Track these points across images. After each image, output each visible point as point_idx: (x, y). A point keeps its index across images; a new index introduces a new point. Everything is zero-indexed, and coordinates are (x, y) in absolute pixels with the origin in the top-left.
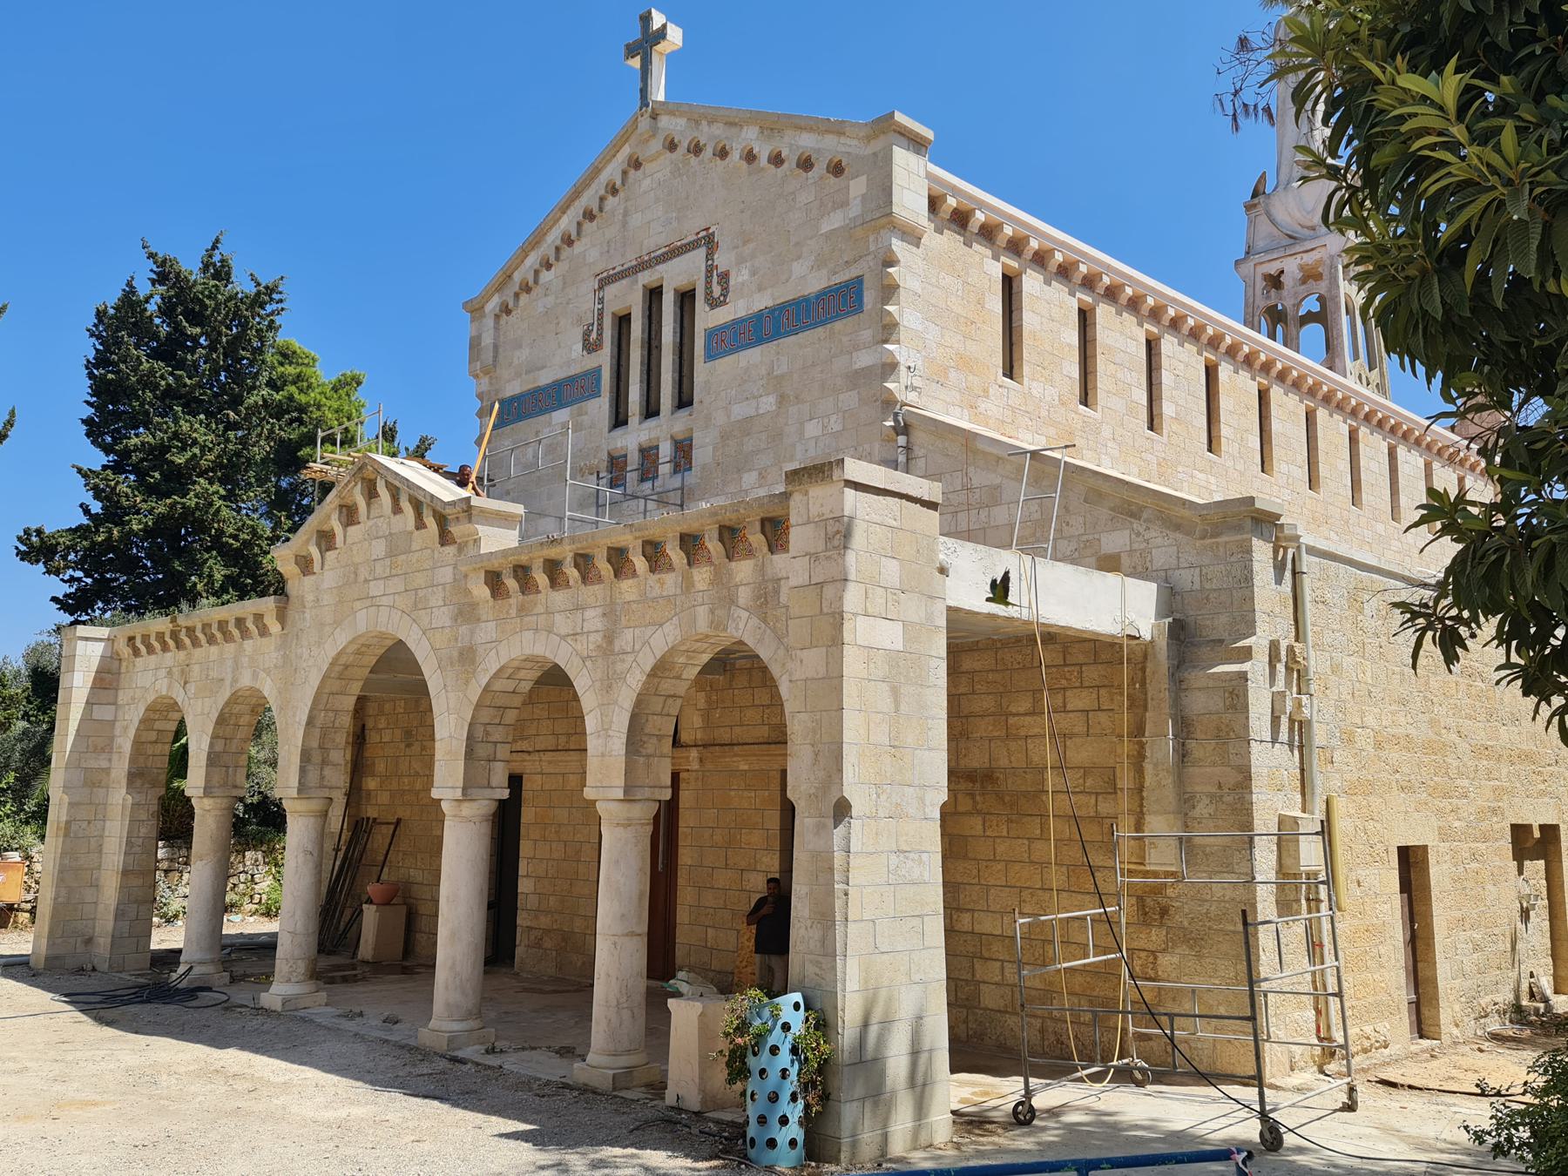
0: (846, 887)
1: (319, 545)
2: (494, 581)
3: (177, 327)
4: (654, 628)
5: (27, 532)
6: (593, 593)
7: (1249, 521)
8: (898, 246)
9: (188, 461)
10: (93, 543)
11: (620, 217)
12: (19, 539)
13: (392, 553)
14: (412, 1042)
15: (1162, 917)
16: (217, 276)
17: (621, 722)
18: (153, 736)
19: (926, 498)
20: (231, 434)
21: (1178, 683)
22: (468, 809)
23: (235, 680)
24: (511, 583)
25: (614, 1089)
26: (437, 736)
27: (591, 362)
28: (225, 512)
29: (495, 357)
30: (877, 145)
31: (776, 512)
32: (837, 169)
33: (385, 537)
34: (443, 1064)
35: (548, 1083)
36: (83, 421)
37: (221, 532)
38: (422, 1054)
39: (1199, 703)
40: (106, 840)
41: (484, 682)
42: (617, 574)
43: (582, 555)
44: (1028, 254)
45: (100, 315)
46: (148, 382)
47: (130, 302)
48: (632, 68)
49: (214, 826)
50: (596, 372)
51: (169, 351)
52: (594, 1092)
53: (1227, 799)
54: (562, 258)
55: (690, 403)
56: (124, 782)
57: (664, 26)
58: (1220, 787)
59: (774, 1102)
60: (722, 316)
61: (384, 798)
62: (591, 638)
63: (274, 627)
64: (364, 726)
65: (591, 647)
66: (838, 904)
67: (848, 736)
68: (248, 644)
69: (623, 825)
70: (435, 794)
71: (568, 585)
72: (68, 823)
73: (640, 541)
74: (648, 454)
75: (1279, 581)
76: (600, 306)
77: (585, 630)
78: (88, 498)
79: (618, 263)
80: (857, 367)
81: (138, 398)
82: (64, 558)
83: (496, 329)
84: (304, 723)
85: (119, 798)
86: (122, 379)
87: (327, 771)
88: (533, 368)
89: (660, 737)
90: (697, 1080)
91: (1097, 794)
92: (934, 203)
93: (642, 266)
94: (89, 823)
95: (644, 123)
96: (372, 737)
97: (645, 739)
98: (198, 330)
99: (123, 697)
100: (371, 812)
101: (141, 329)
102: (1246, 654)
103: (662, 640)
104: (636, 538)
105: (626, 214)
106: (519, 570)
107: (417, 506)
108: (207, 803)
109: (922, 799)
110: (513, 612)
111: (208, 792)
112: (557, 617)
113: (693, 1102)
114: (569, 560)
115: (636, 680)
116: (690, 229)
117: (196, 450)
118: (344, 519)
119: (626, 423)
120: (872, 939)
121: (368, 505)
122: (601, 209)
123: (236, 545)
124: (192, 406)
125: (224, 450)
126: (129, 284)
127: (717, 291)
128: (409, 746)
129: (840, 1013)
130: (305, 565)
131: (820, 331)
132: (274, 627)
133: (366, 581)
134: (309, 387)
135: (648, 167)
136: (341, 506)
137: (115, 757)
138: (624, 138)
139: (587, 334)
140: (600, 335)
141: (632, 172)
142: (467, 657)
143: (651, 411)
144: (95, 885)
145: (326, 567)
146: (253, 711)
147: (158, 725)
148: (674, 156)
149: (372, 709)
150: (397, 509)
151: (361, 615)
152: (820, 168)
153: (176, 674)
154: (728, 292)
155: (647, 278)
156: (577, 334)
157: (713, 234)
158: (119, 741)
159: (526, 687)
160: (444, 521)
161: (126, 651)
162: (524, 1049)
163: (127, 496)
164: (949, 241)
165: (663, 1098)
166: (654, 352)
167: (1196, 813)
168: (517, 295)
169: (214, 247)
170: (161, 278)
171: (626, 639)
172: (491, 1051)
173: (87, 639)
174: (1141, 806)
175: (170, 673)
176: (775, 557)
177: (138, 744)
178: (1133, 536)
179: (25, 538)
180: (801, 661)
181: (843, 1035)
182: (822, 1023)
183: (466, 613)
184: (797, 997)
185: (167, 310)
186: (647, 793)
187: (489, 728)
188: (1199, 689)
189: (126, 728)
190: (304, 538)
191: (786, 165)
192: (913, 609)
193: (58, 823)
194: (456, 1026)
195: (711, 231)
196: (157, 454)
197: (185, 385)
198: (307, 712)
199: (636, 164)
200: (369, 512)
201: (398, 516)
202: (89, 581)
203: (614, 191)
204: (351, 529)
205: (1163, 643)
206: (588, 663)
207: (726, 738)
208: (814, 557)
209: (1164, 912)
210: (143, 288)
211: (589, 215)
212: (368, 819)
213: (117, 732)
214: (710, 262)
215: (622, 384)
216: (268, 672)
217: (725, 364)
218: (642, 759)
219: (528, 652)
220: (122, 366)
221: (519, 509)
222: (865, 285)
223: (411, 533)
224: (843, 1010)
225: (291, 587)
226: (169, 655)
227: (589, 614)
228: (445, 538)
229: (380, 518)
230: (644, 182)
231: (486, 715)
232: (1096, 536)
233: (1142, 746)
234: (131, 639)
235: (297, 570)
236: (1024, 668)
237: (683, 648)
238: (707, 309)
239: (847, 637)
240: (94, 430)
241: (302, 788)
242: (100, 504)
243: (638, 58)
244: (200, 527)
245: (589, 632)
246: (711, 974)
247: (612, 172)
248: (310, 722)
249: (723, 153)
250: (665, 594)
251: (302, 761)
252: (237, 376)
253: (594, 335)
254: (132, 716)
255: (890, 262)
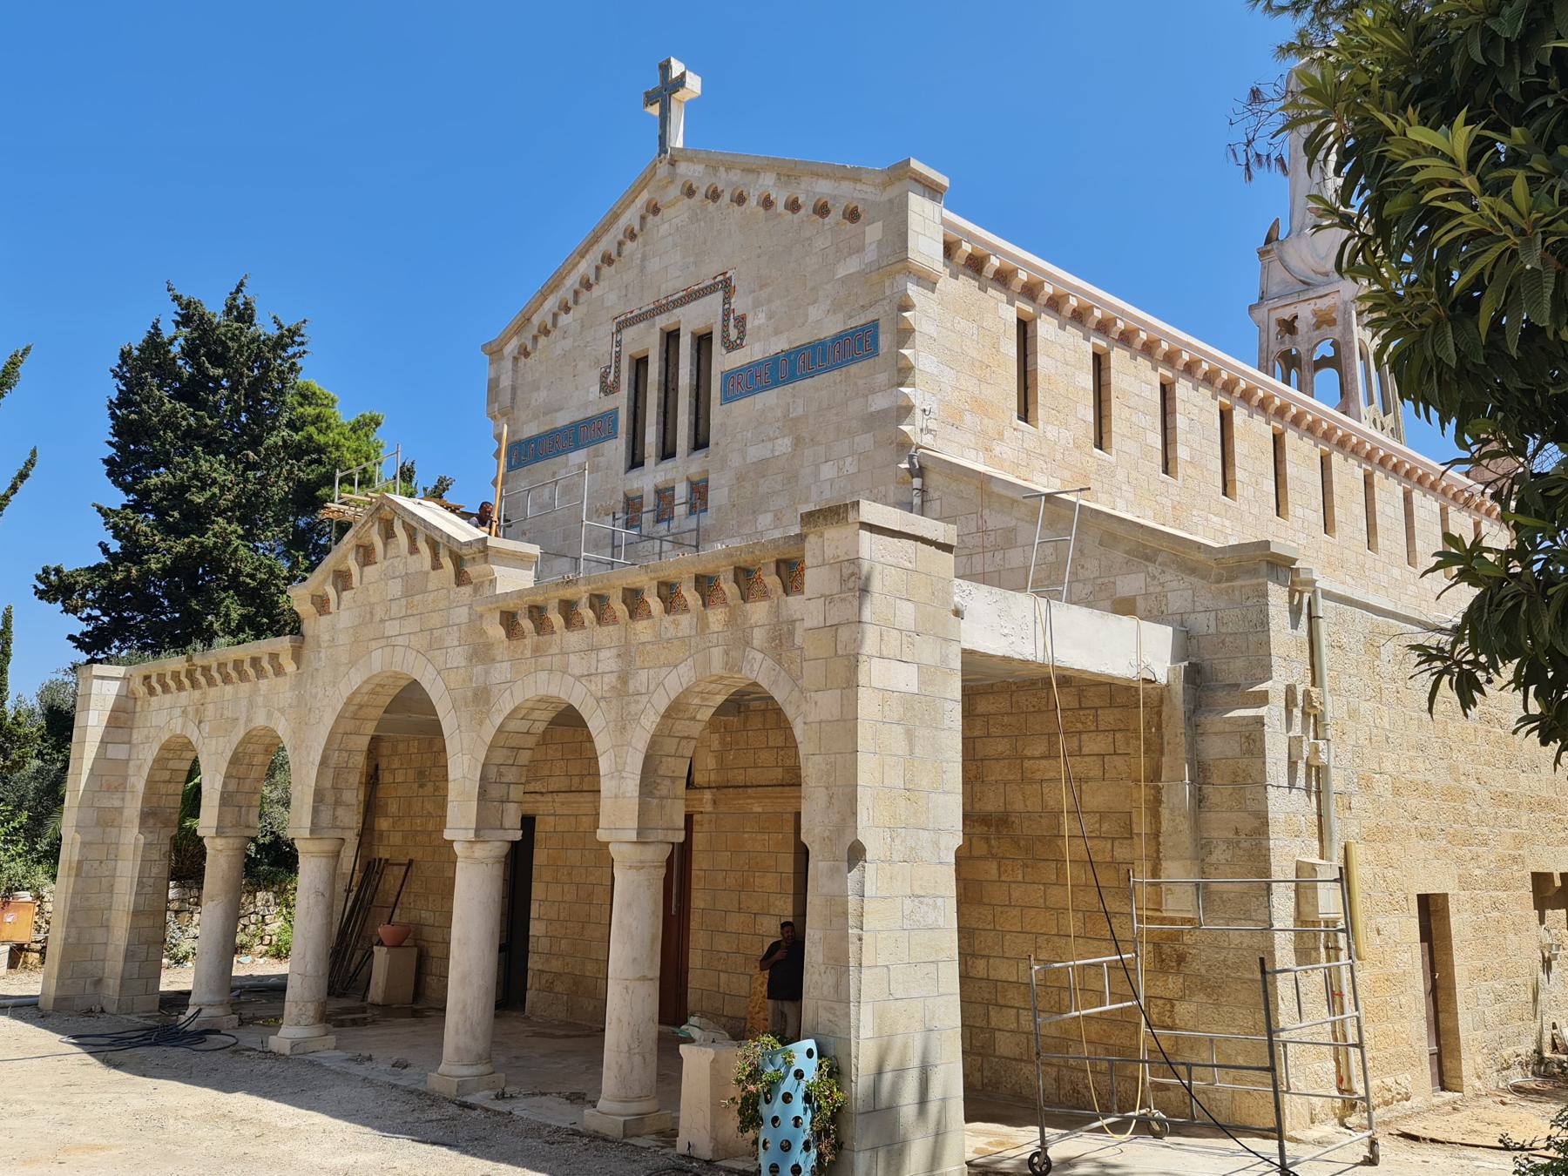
0: (860, 932)
1: (335, 585)
2: (509, 621)
3: (200, 368)
4: (669, 669)
5: (46, 571)
6: (607, 634)
7: (1264, 565)
8: (913, 290)
9: (207, 500)
10: (111, 582)
11: (638, 262)
12: (38, 577)
13: (408, 593)
14: (421, 1087)
15: (1179, 965)
16: (240, 318)
17: (635, 762)
18: (166, 775)
19: (941, 540)
20: (250, 474)
21: (1194, 728)
22: (481, 851)
23: (249, 720)
24: (526, 624)
25: (625, 1136)
26: (451, 777)
27: (608, 403)
28: (242, 552)
29: (513, 399)
30: (892, 192)
31: (790, 553)
32: (853, 215)
33: (401, 577)
34: (452, 1110)
35: (558, 1129)
36: (105, 462)
37: (238, 572)
38: (431, 1099)
39: (1216, 748)
40: (117, 880)
41: (498, 722)
42: (633, 615)
43: (598, 596)
44: (1043, 299)
45: (125, 356)
46: (169, 422)
47: (154, 344)
48: (651, 116)
49: (225, 866)
50: (615, 411)
51: (190, 393)
52: (605, 1139)
53: (1244, 845)
54: (581, 301)
55: (706, 445)
56: (137, 821)
57: (683, 75)
58: (1237, 833)
59: (786, 1151)
60: (738, 359)
61: (396, 839)
63: (290, 667)
64: (377, 766)
65: (606, 688)
66: (852, 949)
67: (863, 779)
68: (263, 684)
69: (636, 867)
70: (448, 835)
71: (583, 626)
72: (80, 862)
73: (655, 582)
74: (664, 495)
75: (1295, 625)
76: (618, 349)
77: (599, 671)
78: (108, 537)
79: (637, 305)
80: (873, 409)
81: (159, 438)
82: (82, 596)
83: (515, 370)
84: (317, 763)
85: (131, 837)
86: (144, 419)
87: (340, 811)
88: (550, 410)
89: (673, 779)
90: (708, 1128)
91: (1113, 839)
92: (949, 249)
93: (660, 309)
94: (101, 863)
95: (663, 169)
96: (386, 777)
97: (659, 781)
98: (221, 371)
99: (137, 736)
100: (383, 853)
101: (165, 370)
102: (1263, 698)
103: (676, 681)
104: (651, 579)
105: (644, 259)
106: (535, 610)
107: (434, 546)
108: (220, 843)
109: (936, 844)
110: (528, 653)
111: (220, 832)
112: (572, 657)
113: (704, 1150)
114: (584, 600)
115: (650, 722)
116: (707, 273)
117: (216, 490)
118: (361, 559)
119: (642, 464)
120: (886, 985)
121: (385, 545)
122: (619, 254)
123: (253, 584)
124: (212, 447)
125: (243, 490)
126: (155, 326)
127: (733, 334)
128: (421, 786)
129: (854, 1061)
130: (321, 604)
131: (836, 375)
132: (290, 667)
133: (382, 621)
134: (328, 427)
135: (666, 213)
136: (358, 546)
137: (128, 796)
138: (643, 184)
139: (604, 376)
140: (617, 377)
141: (650, 218)
142: (481, 698)
143: (667, 453)
144: (106, 927)
145: (342, 607)
146: (267, 751)
147: (172, 764)
148: (692, 201)
149: (385, 748)
150: (414, 549)
151: (377, 656)
152: (836, 214)
153: (191, 715)
154: (744, 336)
155: (664, 321)
157: (730, 278)
158: (133, 779)
159: (540, 727)
160: (460, 561)
161: (141, 690)
162: (534, 1094)
163: (146, 535)
164: (962, 287)
165: (675, 1146)
166: (671, 394)
167: (1213, 859)
168: (535, 338)
169: (238, 290)
170: (185, 320)
171: (640, 680)
172: (501, 1096)
173: (103, 678)
174: (1158, 851)
175: (184, 712)
176: (790, 599)
177: (151, 783)
178: (1148, 580)
179: (44, 576)
180: (816, 703)
181: (856, 1083)
182: (835, 1070)
183: (481, 653)
184: (810, 1044)
185: (190, 352)
186: (660, 835)
187: (503, 769)
188: (1215, 733)
189: (140, 767)
190: (321, 577)
191: (802, 211)
192: (928, 651)
193: (70, 862)
194: (466, 1071)
195: (728, 275)
196: (177, 493)
197: (206, 426)
198: (321, 751)
199: (655, 210)
200: (385, 552)
201: (415, 557)
202: (106, 619)
203: (632, 236)
204: (368, 569)
205: (1179, 687)
206: (603, 704)
207: (740, 780)
208: (828, 598)
209: (1181, 959)
210: (168, 330)
211: (608, 260)
212: (380, 859)
213: (131, 771)
214: (727, 306)
215: (638, 426)
216: (282, 711)
217: (741, 407)
218: (655, 801)
219: (542, 692)
220: (145, 407)
221: (535, 550)
222: (881, 329)
223: (427, 573)
224: (857, 1057)
225: (307, 627)
226: (183, 694)
227: (604, 654)
228: (461, 578)
229: (397, 558)
230: (662, 227)
231: (500, 756)
232: (1112, 580)
233: (1158, 790)
234: (147, 678)
235: (314, 610)
236: (1039, 711)
237: (697, 689)
238: (724, 351)
239: (862, 679)
240: (115, 469)
241: (314, 828)
242: (120, 544)
243: (658, 105)
244: (218, 566)
245: (603, 673)
246: (724, 1020)
247: (630, 217)
248: (324, 762)
249: (740, 199)
250: (680, 635)
251: (314, 801)
252: (257, 416)
253: (611, 378)
254: (147, 754)
255: (906, 306)
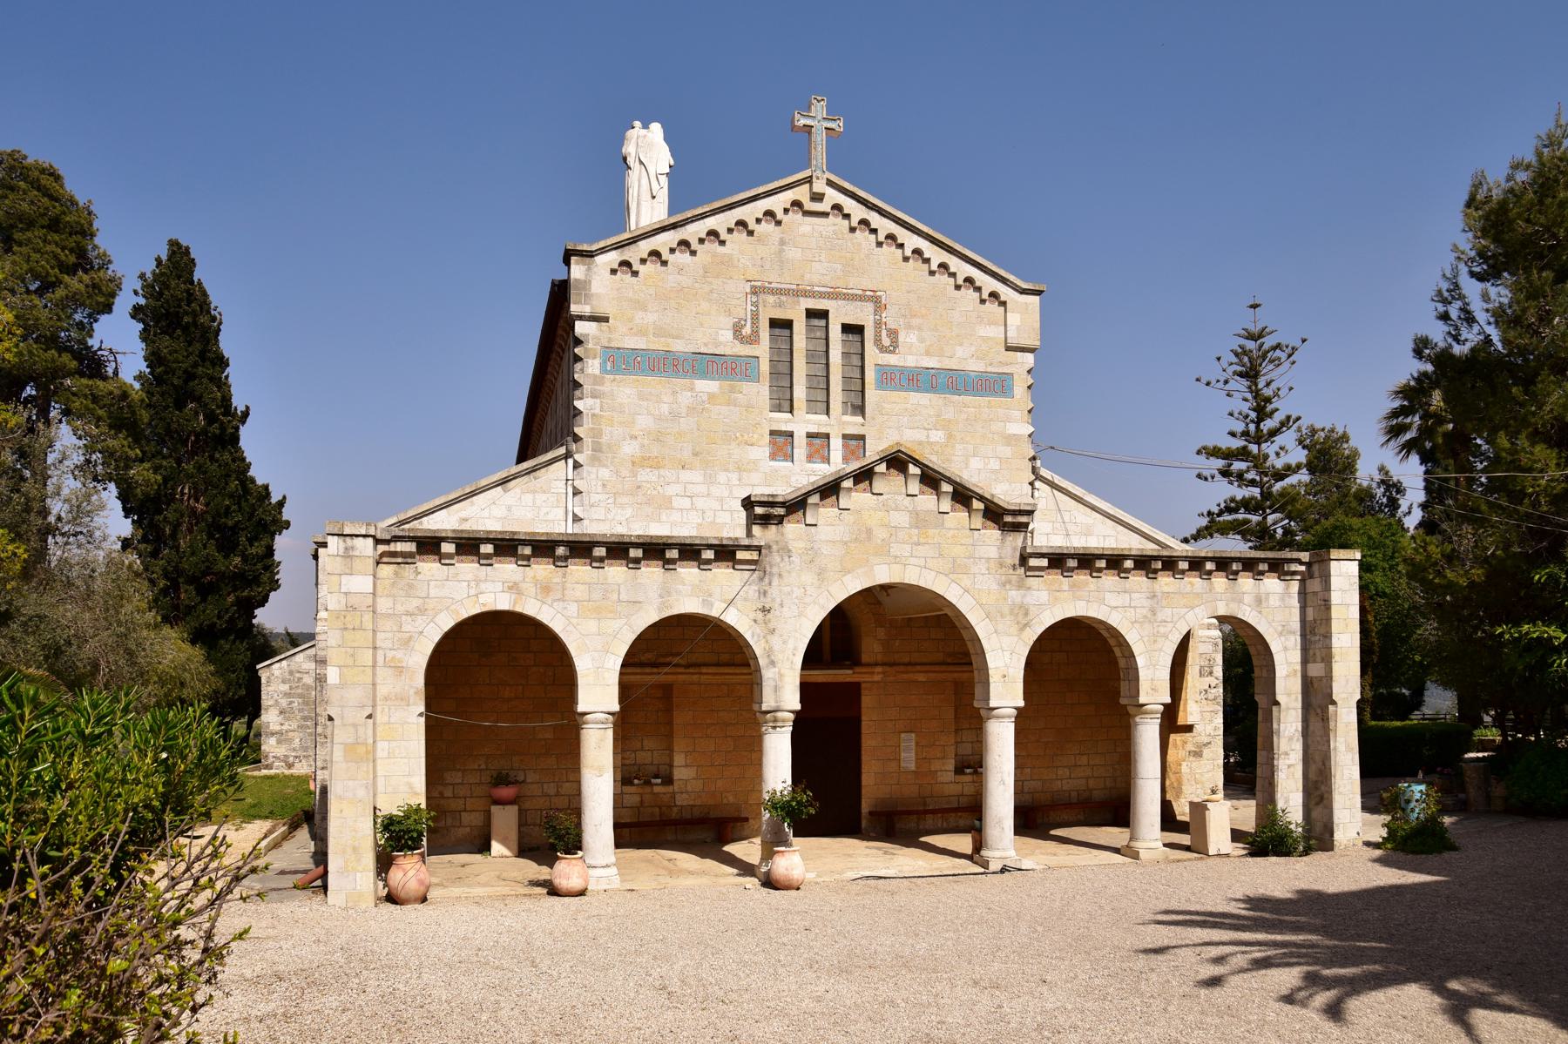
4: (1187, 610)
62: (1138, 610)
80: (1010, 432)
127: (886, 341)
140: (755, 332)
156: (728, 322)
157: (880, 297)
206: (1137, 625)
207: (906, 660)
238: (877, 351)
245: (1135, 607)
253: (747, 330)
